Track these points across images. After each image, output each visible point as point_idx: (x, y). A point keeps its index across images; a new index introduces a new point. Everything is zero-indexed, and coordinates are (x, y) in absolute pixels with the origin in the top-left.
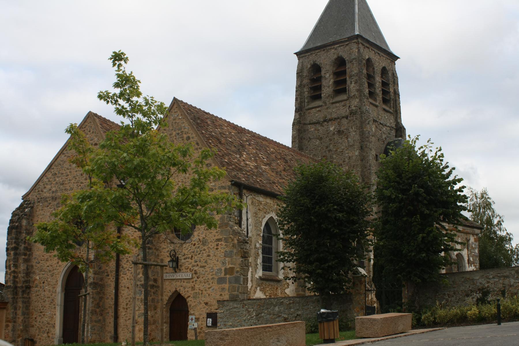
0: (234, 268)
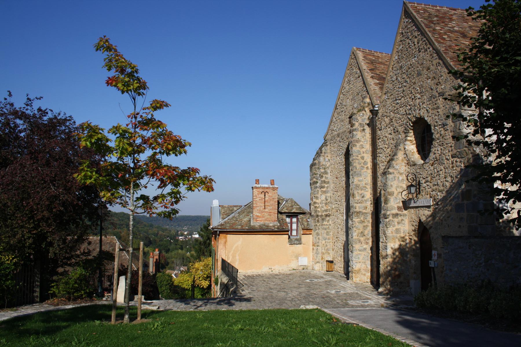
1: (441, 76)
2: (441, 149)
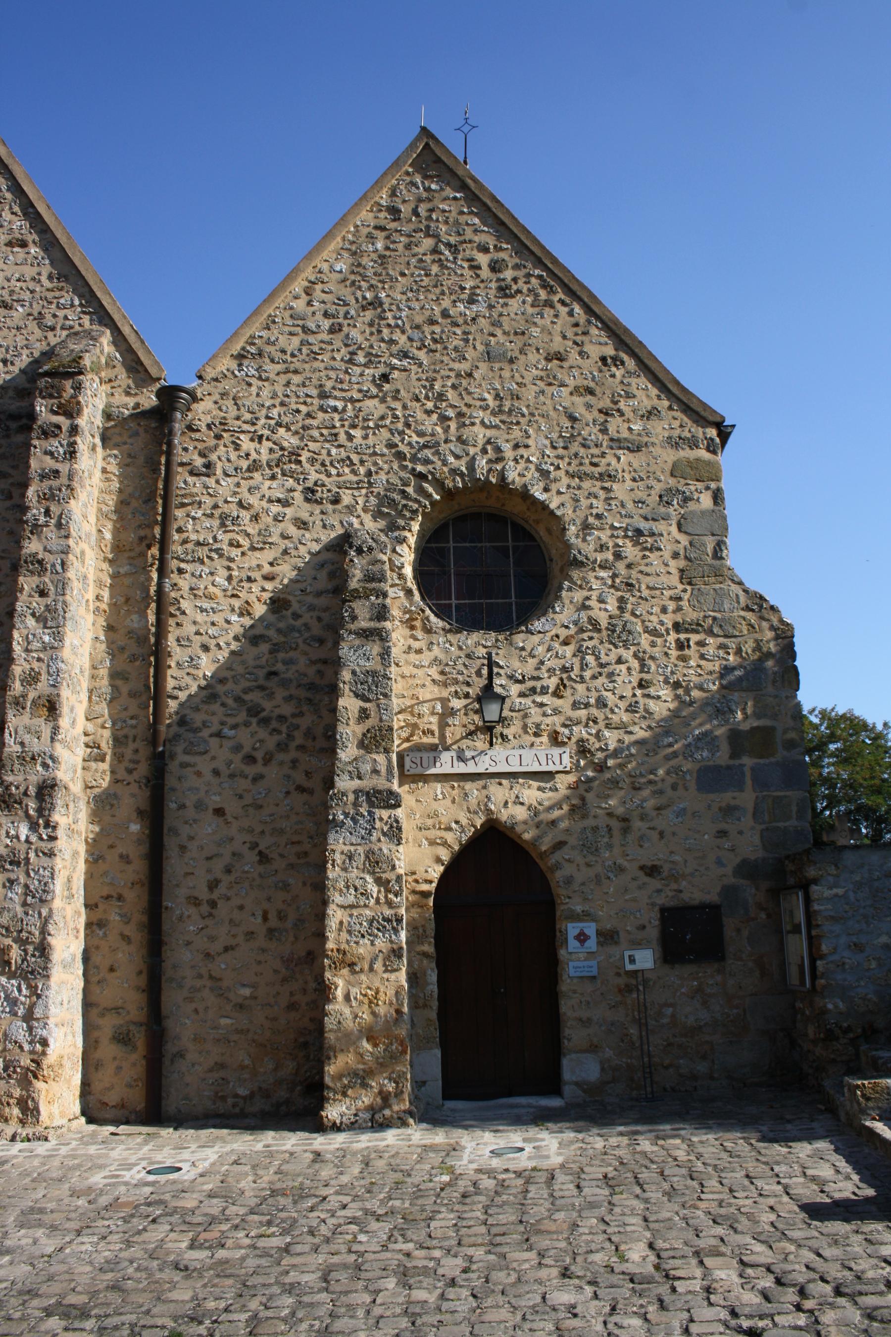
0: (773, 729)
1: (629, 396)
2: (621, 600)
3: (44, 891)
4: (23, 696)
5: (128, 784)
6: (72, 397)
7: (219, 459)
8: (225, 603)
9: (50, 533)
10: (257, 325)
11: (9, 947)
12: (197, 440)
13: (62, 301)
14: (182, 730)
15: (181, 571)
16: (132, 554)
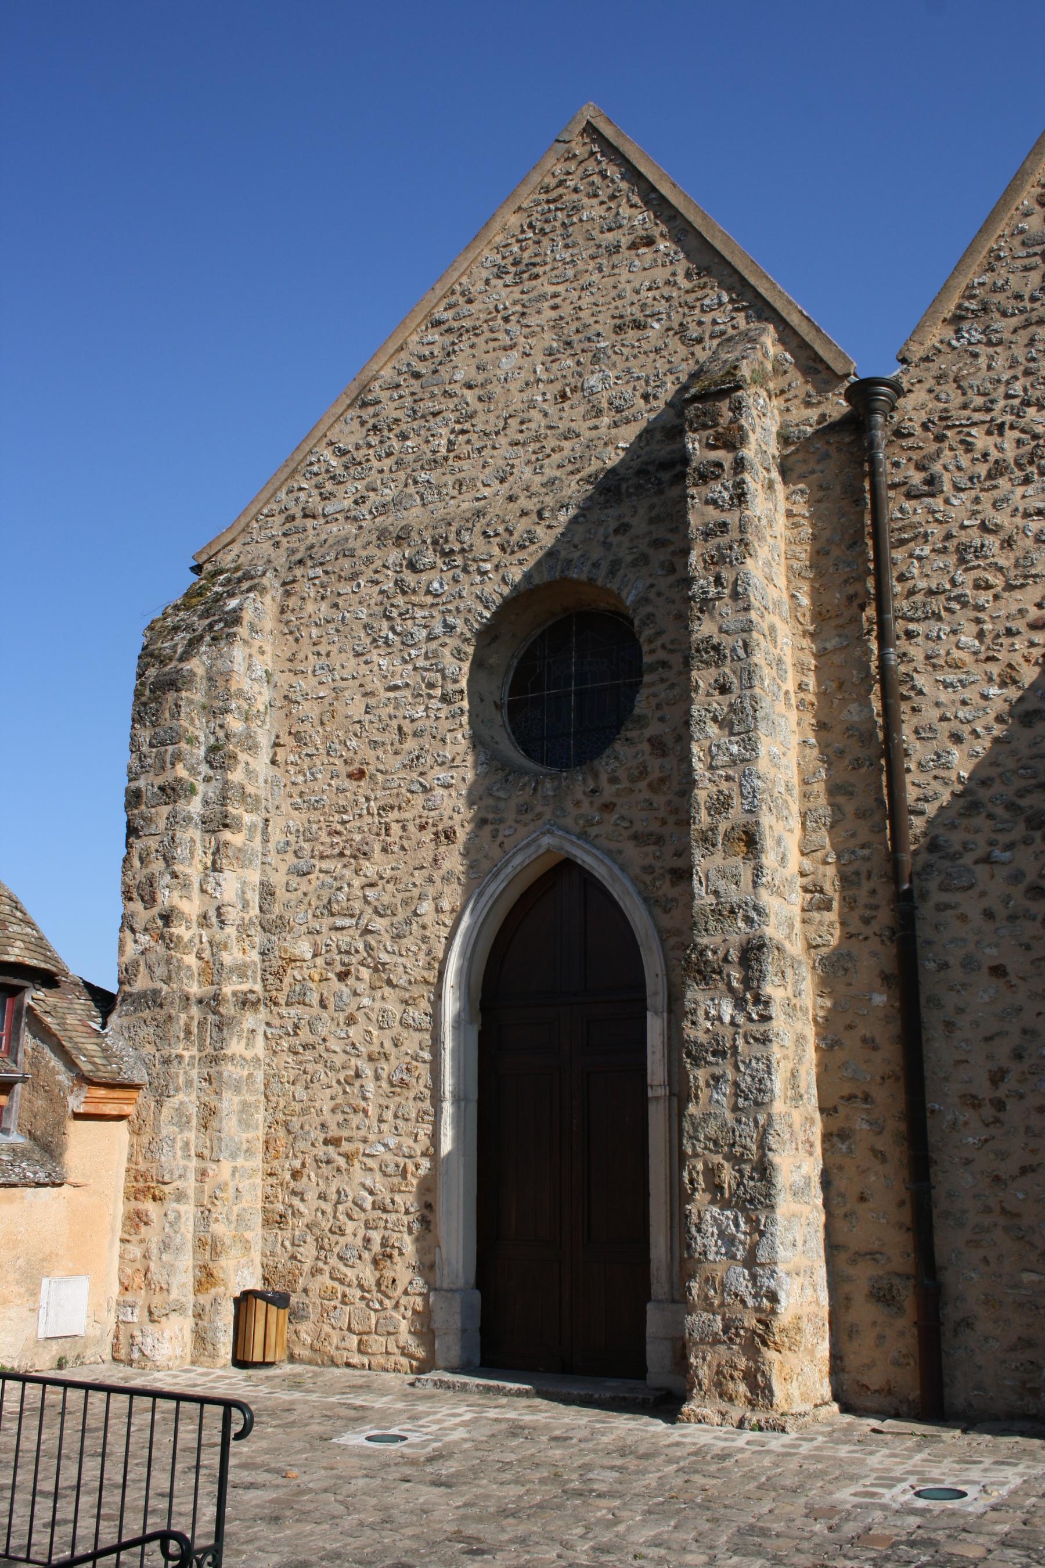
3: (760, 1090)
4: (712, 830)
5: (866, 939)
6: (731, 422)
7: (945, 468)
8: (977, 671)
9: (725, 607)
10: (975, 268)
11: (720, 1166)
12: (910, 448)
13: (707, 302)
14: (933, 858)
15: (910, 635)
16: (840, 621)
